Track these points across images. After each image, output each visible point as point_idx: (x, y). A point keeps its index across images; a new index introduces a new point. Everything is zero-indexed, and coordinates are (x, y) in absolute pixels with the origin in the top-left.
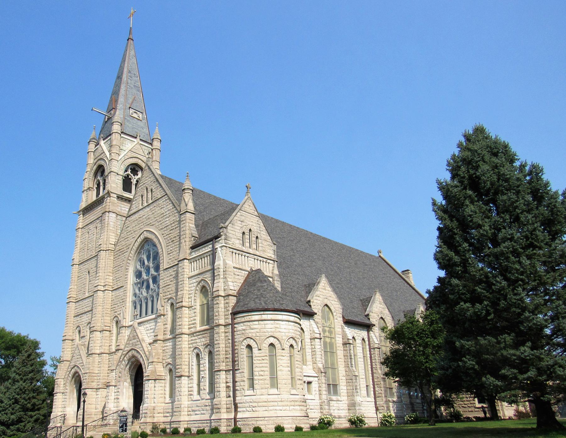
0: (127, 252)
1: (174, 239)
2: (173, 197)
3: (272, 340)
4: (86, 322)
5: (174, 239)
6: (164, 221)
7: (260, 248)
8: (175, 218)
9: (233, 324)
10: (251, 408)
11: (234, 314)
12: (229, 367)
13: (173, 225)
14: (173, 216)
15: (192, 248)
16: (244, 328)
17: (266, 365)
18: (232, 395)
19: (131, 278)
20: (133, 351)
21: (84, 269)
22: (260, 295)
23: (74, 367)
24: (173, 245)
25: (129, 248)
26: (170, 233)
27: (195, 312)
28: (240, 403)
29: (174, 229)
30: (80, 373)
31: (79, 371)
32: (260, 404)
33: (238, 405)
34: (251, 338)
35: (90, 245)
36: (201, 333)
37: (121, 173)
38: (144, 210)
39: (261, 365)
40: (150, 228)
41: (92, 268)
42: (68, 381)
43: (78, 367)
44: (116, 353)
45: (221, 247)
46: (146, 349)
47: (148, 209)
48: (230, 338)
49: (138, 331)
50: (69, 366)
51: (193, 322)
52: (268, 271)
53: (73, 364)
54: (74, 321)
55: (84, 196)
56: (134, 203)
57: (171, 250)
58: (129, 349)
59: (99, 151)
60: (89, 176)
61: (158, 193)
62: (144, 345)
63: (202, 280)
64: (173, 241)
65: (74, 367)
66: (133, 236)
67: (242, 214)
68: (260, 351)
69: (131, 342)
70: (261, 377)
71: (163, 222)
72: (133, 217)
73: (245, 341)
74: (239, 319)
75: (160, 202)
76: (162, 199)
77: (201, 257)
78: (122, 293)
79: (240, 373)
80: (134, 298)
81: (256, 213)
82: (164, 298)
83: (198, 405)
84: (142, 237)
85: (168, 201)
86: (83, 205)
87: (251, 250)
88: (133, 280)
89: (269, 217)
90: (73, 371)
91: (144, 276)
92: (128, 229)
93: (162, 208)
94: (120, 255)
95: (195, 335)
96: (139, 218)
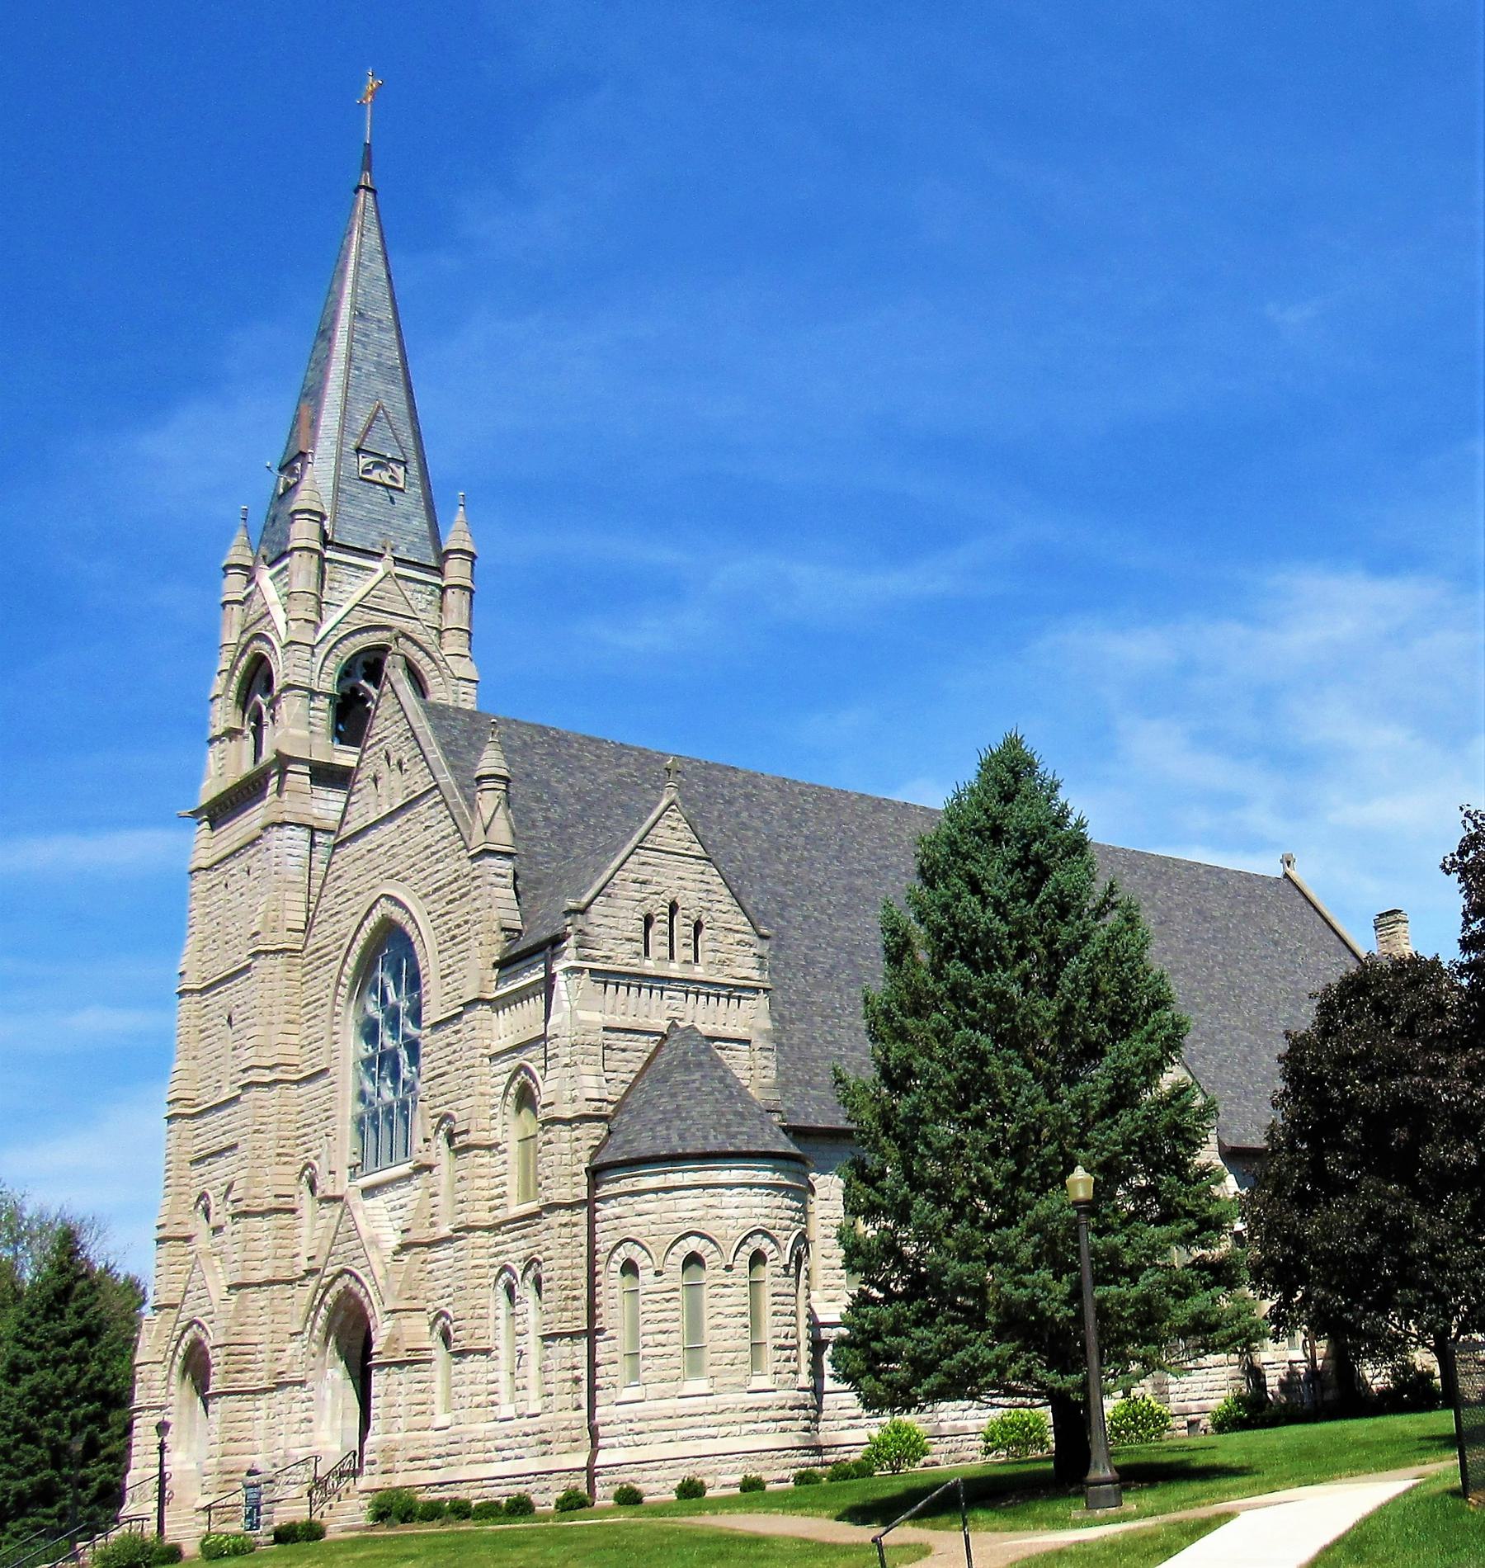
0: (336, 958)
1: (456, 931)
2: (454, 796)
3: (693, 1244)
4: (222, 1180)
5: (456, 931)
6: (430, 870)
9: (590, 1204)
11: (596, 1173)
12: (579, 1323)
13: (454, 886)
14: (455, 857)
15: (501, 965)
16: (618, 1211)
17: (676, 1314)
18: (585, 1405)
19: (353, 1047)
20: (347, 1276)
22: (673, 1111)
23: (189, 1326)
24: (455, 950)
25: (341, 946)
26: (448, 913)
27: (504, 1163)
28: (603, 1425)
30: (208, 1344)
31: (203, 1336)
32: (655, 1424)
33: (600, 1429)
34: (636, 1242)
35: (231, 929)
37: (329, 685)
39: (661, 1316)
40: (395, 887)
41: (238, 1006)
42: (176, 1369)
43: (200, 1325)
44: (305, 1282)
45: (566, 971)
46: (379, 1271)
48: (584, 1239)
49: (359, 1215)
50: (177, 1322)
51: (500, 1190)
53: (186, 1315)
54: (193, 1174)
55: (213, 754)
57: (449, 966)
58: (336, 1269)
59: (256, 609)
60: (227, 689)
61: (417, 778)
62: (374, 1257)
63: (522, 1067)
64: (453, 938)
65: (189, 1326)
67: (643, 859)
68: (660, 1278)
69: (341, 1249)
70: (660, 1350)
72: (351, 849)
74: (605, 1187)
75: (422, 807)
77: (521, 996)
79: (605, 1340)
80: (360, 1108)
81: (698, 847)
82: (432, 1113)
83: (507, 1432)
84: (376, 915)
85: (442, 806)
86: (210, 789)
88: (356, 1050)
89: (847, 795)
90: (188, 1336)
91: (387, 1040)
93: (427, 827)
94: (319, 968)
95: (503, 1228)
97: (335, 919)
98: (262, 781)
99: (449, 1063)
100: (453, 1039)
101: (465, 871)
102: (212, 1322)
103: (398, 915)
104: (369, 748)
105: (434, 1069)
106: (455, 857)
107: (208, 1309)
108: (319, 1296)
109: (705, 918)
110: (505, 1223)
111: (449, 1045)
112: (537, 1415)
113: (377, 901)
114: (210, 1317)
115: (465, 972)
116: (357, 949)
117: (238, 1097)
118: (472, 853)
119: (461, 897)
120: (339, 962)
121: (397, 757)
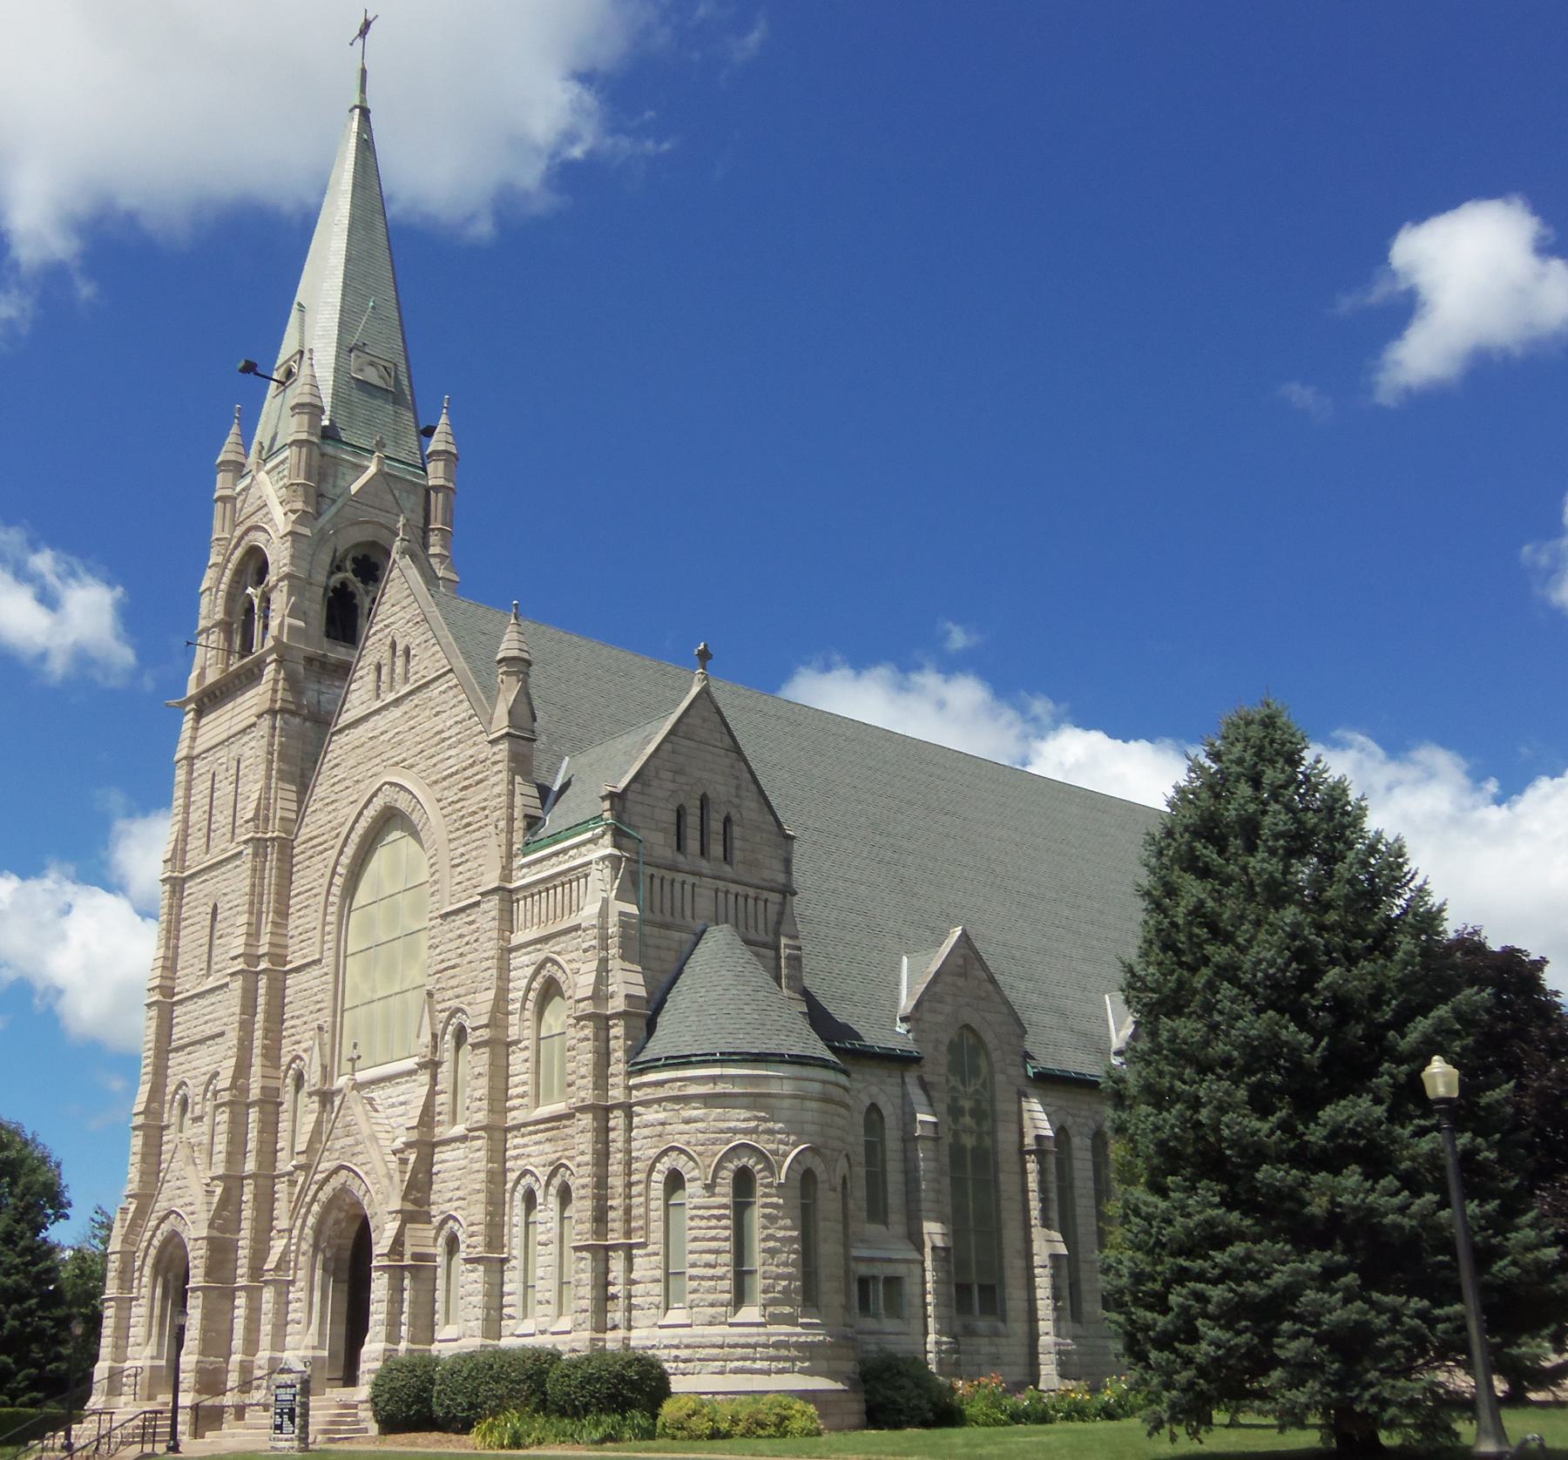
0: (332, 847)
4: (203, 1070)
6: (441, 757)
7: (737, 855)
8: (476, 748)
10: (674, 1365)
21: (201, 895)
23: (166, 1217)
24: (468, 838)
29: (470, 786)
32: (703, 1353)
34: (682, 1151)
36: (542, 1127)
38: (384, 713)
40: (400, 775)
41: (225, 894)
47: (396, 712)
52: (761, 926)
56: (353, 687)
62: (374, 1154)
63: (548, 960)
64: (469, 825)
65: (166, 1217)
66: (351, 799)
70: (710, 1272)
71: (442, 761)
73: (665, 1159)
76: (437, 683)
78: (317, 982)
79: (648, 1255)
84: (378, 803)
87: (704, 863)
92: (335, 771)
94: (312, 857)
96: (371, 738)
97: (331, 808)
98: (256, 671)
99: (461, 955)
100: (464, 930)
101: (482, 757)
102: (192, 1213)
103: (402, 802)
104: (374, 634)
105: (443, 961)
106: (470, 742)
107: (187, 1200)
108: (311, 1193)
109: (735, 817)
110: (525, 1125)
111: (461, 936)
112: (569, 1332)
113: (380, 789)
114: (190, 1209)
115: (480, 861)
116: (355, 839)
117: (226, 985)
118: (492, 737)
119: (477, 784)
120: (336, 851)
121: (404, 644)
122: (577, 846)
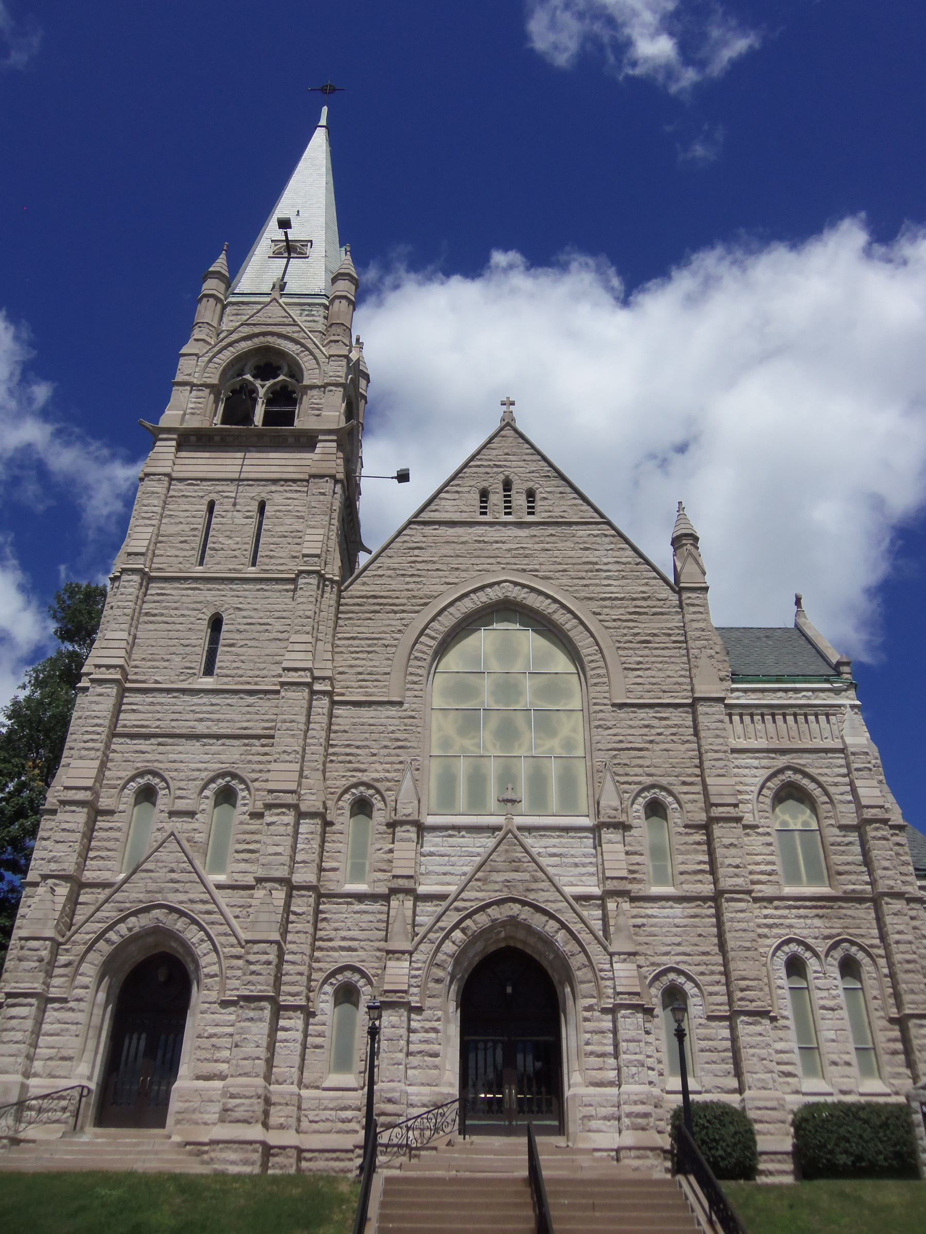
13: (638, 603)
36: (808, 903)
71: (597, 585)
122: (813, 690)
